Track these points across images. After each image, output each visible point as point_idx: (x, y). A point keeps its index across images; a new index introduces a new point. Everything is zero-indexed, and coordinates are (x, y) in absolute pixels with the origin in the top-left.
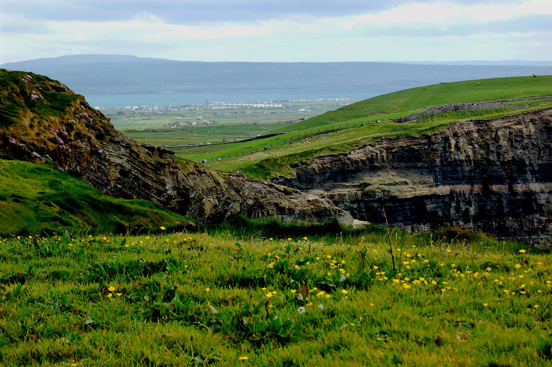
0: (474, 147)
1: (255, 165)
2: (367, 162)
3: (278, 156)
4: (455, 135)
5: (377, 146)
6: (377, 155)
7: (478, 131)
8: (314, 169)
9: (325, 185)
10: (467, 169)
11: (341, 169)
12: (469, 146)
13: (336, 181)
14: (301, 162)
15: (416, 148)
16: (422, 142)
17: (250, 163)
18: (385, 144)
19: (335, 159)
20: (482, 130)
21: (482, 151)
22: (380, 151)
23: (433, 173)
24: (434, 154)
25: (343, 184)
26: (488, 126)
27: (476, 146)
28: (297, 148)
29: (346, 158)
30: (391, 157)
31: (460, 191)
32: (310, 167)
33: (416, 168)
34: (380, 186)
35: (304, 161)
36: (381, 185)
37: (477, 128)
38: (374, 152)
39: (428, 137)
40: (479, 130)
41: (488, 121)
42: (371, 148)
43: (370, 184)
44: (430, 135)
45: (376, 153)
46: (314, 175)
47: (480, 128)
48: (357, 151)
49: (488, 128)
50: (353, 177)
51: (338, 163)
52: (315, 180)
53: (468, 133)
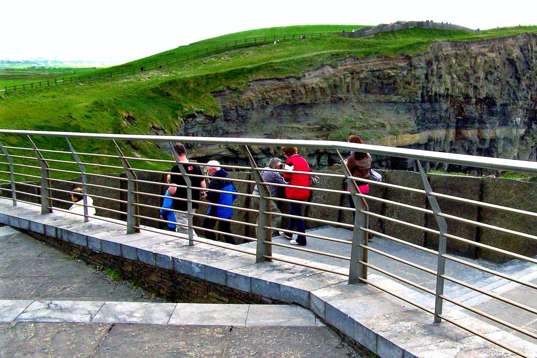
0: (453, 78)
1: (154, 90)
2: (328, 92)
3: (188, 76)
4: (437, 59)
5: (339, 68)
6: (341, 81)
7: (456, 56)
8: (250, 100)
9: (265, 127)
10: (445, 106)
11: (290, 101)
12: (447, 76)
13: (281, 121)
14: (229, 88)
15: (393, 74)
16: (400, 64)
17: (142, 88)
18: (350, 64)
19: (282, 84)
20: (460, 54)
21: (459, 84)
22: (344, 75)
23: (413, 112)
24: (415, 83)
25: (294, 125)
26: (467, 50)
27: (454, 76)
28: (214, 65)
29: (299, 83)
30: (357, 85)
31: (437, 138)
32: (244, 97)
33: (389, 102)
34: (353, 131)
35: (233, 86)
36: (352, 128)
37: (455, 52)
38: (337, 76)
39: (409, 58)
40: (456, 54)
41: (467, 43)
42: (331, 70)
43: (335, 128)
44: (411, 55)
45: (340, 78)
46: (248, 109)
47: (458, 52)
48: (313, 74)
49: (468, 53)
50: (307, 114)
51: (287, 91)
52: (250, 118)
53: (447, 58)
